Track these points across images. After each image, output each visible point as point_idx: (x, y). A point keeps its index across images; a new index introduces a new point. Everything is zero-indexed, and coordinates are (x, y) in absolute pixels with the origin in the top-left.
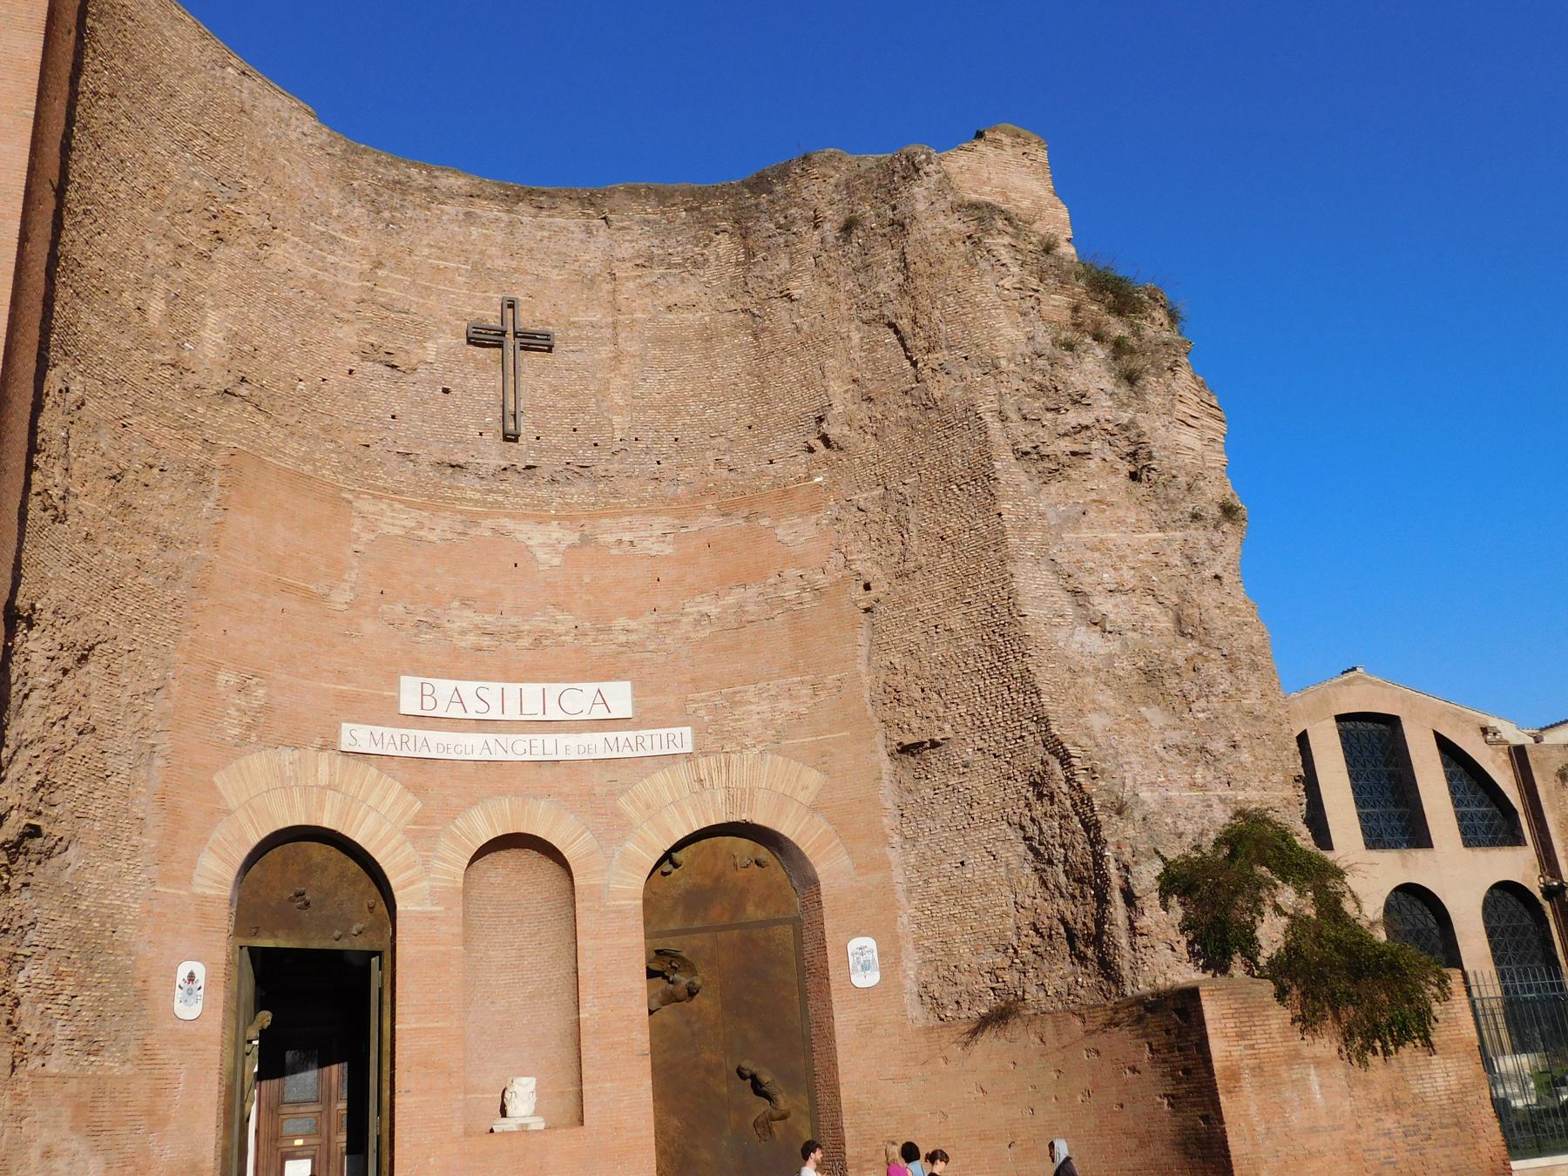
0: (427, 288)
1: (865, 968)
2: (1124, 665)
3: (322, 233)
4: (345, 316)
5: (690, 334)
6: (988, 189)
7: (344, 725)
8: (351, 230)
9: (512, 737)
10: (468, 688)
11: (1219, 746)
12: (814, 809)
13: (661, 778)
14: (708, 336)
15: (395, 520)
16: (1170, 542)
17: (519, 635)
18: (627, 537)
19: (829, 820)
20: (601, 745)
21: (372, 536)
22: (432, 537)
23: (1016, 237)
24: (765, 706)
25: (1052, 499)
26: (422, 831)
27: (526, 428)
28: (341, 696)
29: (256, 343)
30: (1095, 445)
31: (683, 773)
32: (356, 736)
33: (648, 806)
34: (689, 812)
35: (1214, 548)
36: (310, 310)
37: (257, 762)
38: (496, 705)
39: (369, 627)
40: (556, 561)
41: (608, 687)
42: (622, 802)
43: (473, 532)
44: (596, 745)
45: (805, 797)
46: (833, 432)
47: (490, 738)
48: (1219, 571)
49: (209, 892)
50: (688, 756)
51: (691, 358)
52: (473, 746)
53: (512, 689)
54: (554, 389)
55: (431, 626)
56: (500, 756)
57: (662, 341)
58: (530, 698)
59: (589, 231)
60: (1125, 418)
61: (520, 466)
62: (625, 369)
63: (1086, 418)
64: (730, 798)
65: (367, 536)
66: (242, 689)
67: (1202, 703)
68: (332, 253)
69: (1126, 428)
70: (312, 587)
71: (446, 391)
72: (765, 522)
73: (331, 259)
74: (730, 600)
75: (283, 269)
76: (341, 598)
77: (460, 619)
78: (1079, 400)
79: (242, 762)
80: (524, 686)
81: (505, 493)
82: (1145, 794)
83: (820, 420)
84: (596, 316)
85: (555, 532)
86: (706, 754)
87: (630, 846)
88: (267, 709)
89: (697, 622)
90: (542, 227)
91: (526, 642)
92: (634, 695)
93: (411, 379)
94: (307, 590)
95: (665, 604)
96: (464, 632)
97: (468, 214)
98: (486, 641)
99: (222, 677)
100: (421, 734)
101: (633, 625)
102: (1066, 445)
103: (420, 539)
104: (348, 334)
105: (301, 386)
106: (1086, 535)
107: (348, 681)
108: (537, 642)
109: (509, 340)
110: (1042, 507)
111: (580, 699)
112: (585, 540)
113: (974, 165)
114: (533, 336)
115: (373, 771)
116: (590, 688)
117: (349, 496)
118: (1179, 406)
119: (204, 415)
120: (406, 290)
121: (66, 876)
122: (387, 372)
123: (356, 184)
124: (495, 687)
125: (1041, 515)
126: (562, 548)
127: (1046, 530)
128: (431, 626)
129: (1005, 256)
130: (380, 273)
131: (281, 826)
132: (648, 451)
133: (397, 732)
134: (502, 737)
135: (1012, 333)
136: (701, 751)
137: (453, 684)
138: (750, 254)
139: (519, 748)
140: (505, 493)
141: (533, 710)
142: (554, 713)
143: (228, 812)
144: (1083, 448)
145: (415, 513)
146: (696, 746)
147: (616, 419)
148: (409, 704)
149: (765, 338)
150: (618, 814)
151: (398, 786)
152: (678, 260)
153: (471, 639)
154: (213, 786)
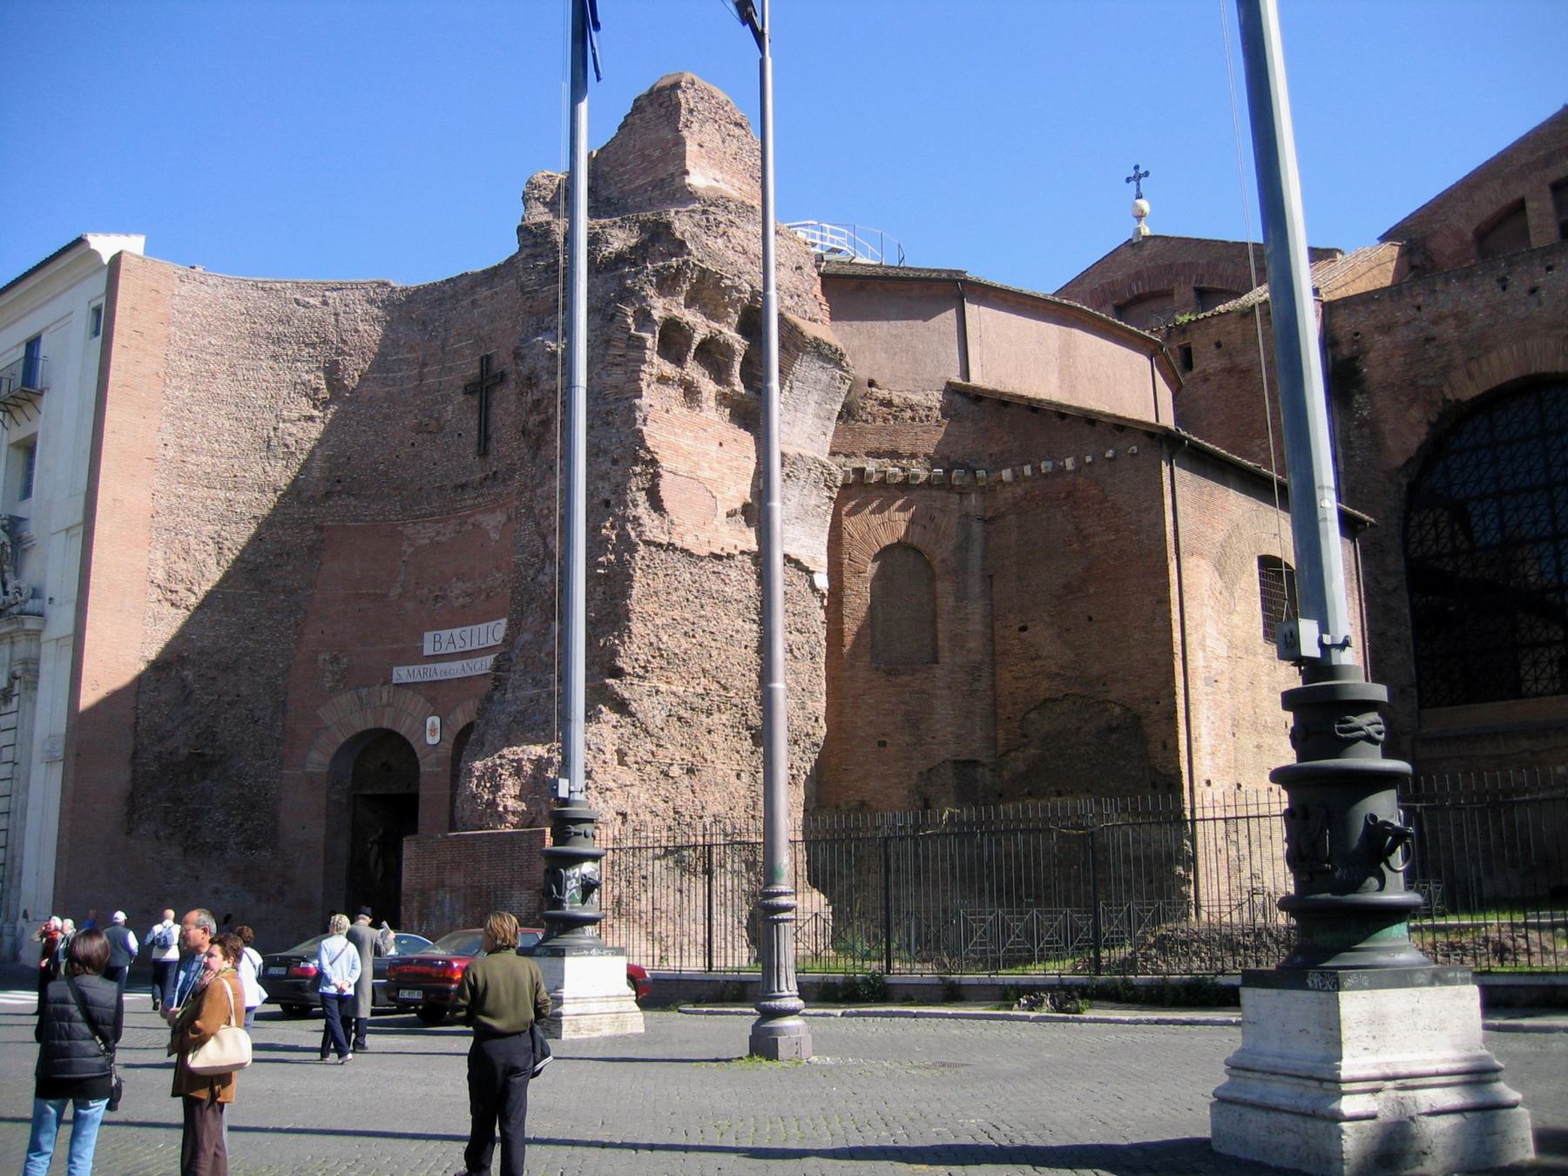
0: (450, 368)
3: (395, 360)
6: (631, 157)
7: (395, 669)
9: (474, 660)
10: (456, 631)
15: (424, 533)
21: (413, 549)
22: (444, 539)
27: (493, 445)
29: (348, 454)
32: (402, 674)
36: (387, 417)
37: (345, 700)
38: (468, 641)
43: (463, 529)
49: (315, 770)
56: (469, 673)
61: (491, 473)
65: (410, 550)
68: (400, 370)
70: (378, 591)
71: (460, 435)
75: (367, 398)
76: (394, 593)
77: (457, 588)
79: (335, 701)
80: (480, 626)
94: (376, 594)
98: (468, 600)
99: (321, 657)
100: (432, 666)
103: (438, 543)
104: (410, 421)
105: (381, 467)
115: (411, 693)
117: (400, 528)
119: (313, 513)
123: (414, 316)
124: (468, 629)
126: (500, 527)
130: (425, 370)
131: (359, 730)
133: (421, 667)
143: (327, 728)
148: (428, 650)
151: (422, 700)
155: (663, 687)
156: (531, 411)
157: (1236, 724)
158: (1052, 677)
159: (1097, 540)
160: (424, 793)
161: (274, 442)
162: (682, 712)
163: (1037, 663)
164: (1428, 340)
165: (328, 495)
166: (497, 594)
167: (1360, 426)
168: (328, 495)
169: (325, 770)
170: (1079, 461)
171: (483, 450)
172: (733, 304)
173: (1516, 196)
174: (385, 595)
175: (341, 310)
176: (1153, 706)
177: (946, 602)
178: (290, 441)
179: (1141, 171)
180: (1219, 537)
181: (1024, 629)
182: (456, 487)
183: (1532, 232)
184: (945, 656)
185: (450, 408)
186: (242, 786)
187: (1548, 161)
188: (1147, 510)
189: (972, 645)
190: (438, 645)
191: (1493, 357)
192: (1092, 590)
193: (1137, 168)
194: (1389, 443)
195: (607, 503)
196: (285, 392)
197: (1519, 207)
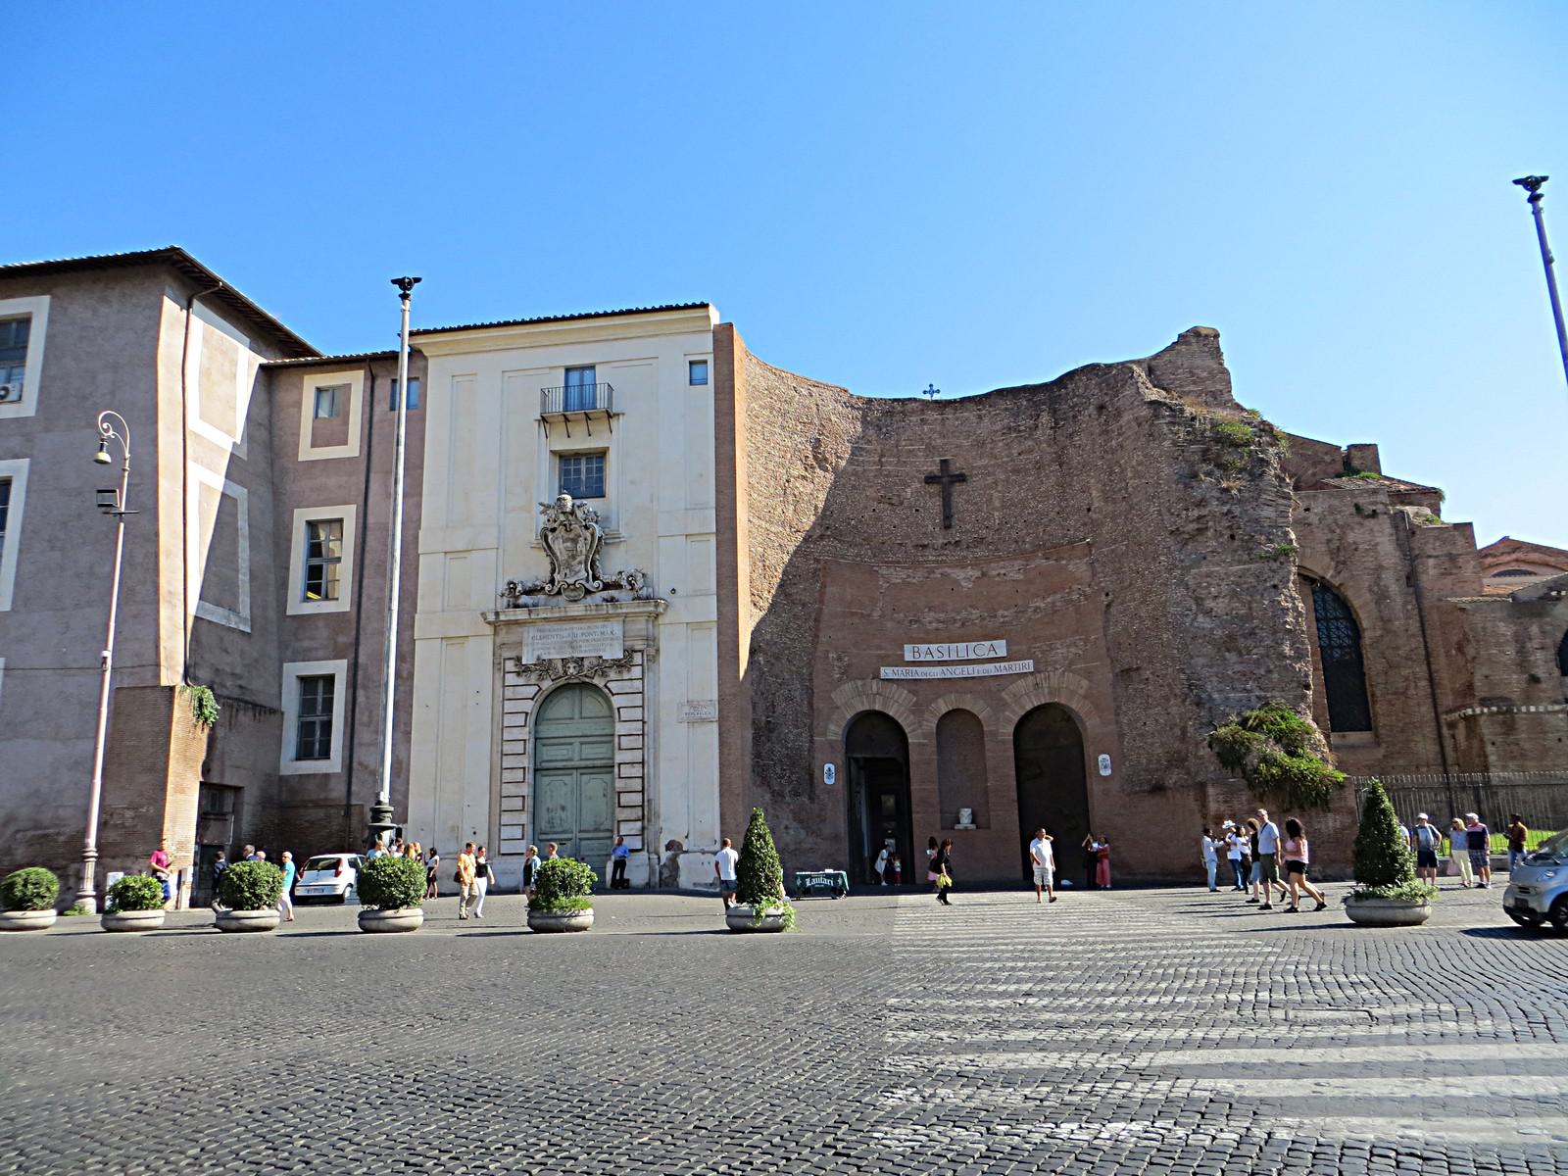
1: (1106, 767)
2: (1218, 633)
5: (1030, 466)
8: (869, 442)
10: (933, 647)
12: (1085, 697)
13: (1021, 683)
14: (1039, 466)
15: (898, 575)
16: (1248, 570)
17: (955, 621)
18: (1003, 572)
19: (1092, 703)
23: (1174, 416)
24: (1065, 650)
26: (917, 710)
27: (955, 521)
28: (878, 656)
30: (1210, 524)
31: (1031, 678)
32: (887, 672)
33: (1015, 696)
34: (1033, 699)
35: (1274, 571)
36: (854, 487)
37: (848, 687)
39: (889, 625)
41: (994, 642)
42: (1003, 694)
44: (991, 669)
45: (1082, 692)
46: (1094, 516)
47: (944, 668)
48: (1276, 582)
50: (1032, 673)
51: (1031, 478)
52: (937, 672)
54: (967, 502)
55: (916, 621)
56: (949, 676)
57: (1016, 471)
58: (961, 650)
59: (980, 417)
60: (1225, 509)
62: (999, 488)
63: (1204, 512)
64: (1050, 693)
66: (839, 659)
67: (1255, 651)
68: (862, 455)
69: (1226, 514)
72: (1064, 562)
73: (861, 459)
74: (1049, 600)
76: (876, 615)
77: (930, 616)
81: (946, 555)
82: (1216, 696)
83: (1089, 510)
84: (985, 462)
85: (970, 572)
86: (1039, 672)
87: (1007, 713)
88: (848, 666)
89: (1035, 611)
90: (957, 419)
91: (958, 625)
95: (1020, 602)
96: (930, 623)
97: (922, 420)
98: (941, 625)
99: (831, 655)
101: (1006, 613)
106: (1204, 569)
107: (881, 649)
108: (963, 624)
109: (945, 480)
111: (983, 649)
112: (984, 574)
113: (1173, 359)
114: (957, 476)
116: (988, 644)
118: (1264, 496)
120: (896, 465)
121: (782, 736)
124: (946, 646)
125: (1182, 561)
127: (1182, 568)
128: (916, 621)
129: (1165, 429)
132: (1012, 527)
134: (949, 668)
135: (1167, 470)
136: (1037, 671)
137: (926, 646)
138: (1056, 423)
139: (959, 672)
140: (946, 555)
141: (963, 655)
142: (972, 656)
143: (838, 708)
147: (996, 514)
148: (908, 657)
149: (1065, 466)
150: (1002, 699)
152: (1022, 428)
154: (830, 697)
160: (913, 757)
161: (788, 491)
165: (822, 537)
166: (975, 624)
168: (822, 537)
169: (840, 738)
171: (947, 526)
174: (869, 615)
175: (819, 403)
178: (796, 493)
179: (935, 388)
182: (916, 546)
185: (908, 490)
186: (787, 748)
190: (917, 655)
193: (931, 386)
196: (789, 456)
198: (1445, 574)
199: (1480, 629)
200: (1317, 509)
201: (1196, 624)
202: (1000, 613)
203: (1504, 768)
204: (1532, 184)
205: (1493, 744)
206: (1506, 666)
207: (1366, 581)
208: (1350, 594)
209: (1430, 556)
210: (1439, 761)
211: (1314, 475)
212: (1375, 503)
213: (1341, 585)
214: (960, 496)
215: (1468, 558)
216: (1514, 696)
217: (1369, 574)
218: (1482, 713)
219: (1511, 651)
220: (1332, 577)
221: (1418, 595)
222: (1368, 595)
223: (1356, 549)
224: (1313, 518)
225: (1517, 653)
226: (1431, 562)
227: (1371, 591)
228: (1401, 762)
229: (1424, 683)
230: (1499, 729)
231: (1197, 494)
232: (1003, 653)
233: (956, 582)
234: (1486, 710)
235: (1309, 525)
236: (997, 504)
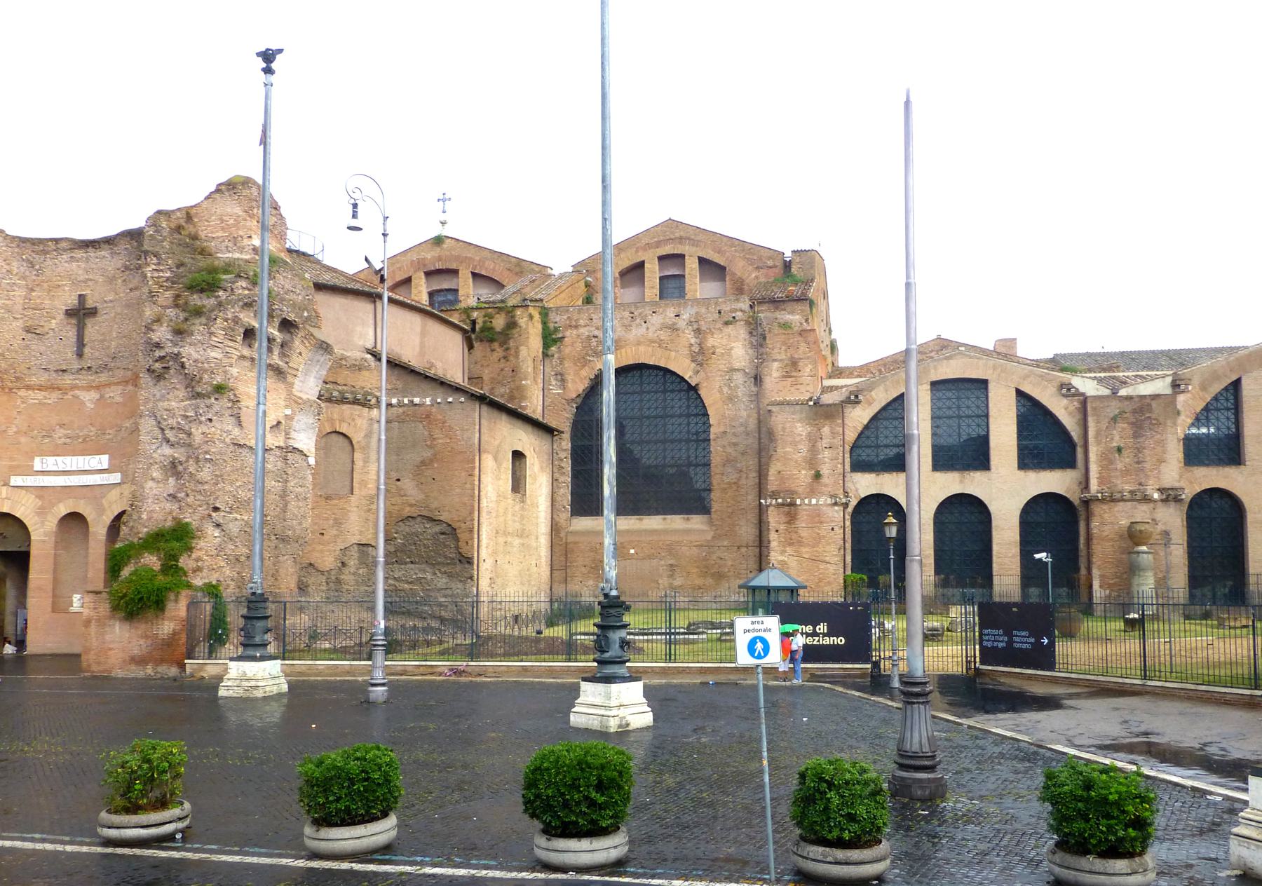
4: (20, 316)
10: (60, 459)
11: (182, 495)
17: (78, 437)
20: (99, 479)
22: (49, 402)
25: (157, 391)
30: (171, 363)
40: (92, 406)
41: (103, 457)
42: (104, 501)
48: (210, 416)
53: (75, 458)
55: (48, 437)
77: (60, 432)
78: (158, 345)
81: (79, 379)
91: (80, 440)
92: (109, 460)
93: (46, 337)
98: (68, 440)
102: (158, 365)
108: (84, 440)
110: (156, 392)
112: (102, 397)
116: (97, 457)
122: (36, 337)
124: (69, 458)
125: (154, 396)
142: (87, 468)
144: (167, 365)
145: (43, 393)
146: (122, 480)
153: (63, 440)
155: (239, 517)
156: (157, 361)
157: (497, 533)
158: (411, 505)
159: (440, 441)
162: (246, 529)
163: (405, 498)
164: (595, 337)
166: (92, 440)
167: (556, 375)
170: (434, 403)
171: (80, 355)
172: (278, 316)
173: (642, 259)
176: (463, 525)
177: (359, 463)
180: (497, 443)
181: (398, 480)
182: (56, 371)
183: (646, 279)
184: (356, 491)
187: (658, 244)
188: (467, 430)
189: (370, 486)
191: (623, 351)
192: (436, 465)
194: (570, 385)
195: (210, 420)
197: (641, 265)
198: (787, 376)
199: (779, 429)
200: (685, 316)
201: (159, 451)
202: (108, 431)
203: (783, 552)
204: (268, 57)
205: (777, 531)
206: (796, 462)
207: (718, 381)
208: (702, 393)
209: (775, 360)
210: (757, 543)
211: (757, 277)
212: (735, 311)
213: (697, 385)
214: (93, 329)
215: (806, 362)
216: (800, 490)
217: (721, 376)
218: (771, 504)
219: (804, 449)
220: (690, 377)
221: (757, 397)
222: (718, 395)
223: (714, 353)
224: (681, 323)
225: (808, 451)
226: (776, 365)
227: (721, 391)
228: (726, 543)
229: (755, 474)
230: (783, 519)
231: (155, 337)
232: (105, 466)
233: (83, 403)
234: (774, 501)
235: (677, 330)
236: (114, 334)
